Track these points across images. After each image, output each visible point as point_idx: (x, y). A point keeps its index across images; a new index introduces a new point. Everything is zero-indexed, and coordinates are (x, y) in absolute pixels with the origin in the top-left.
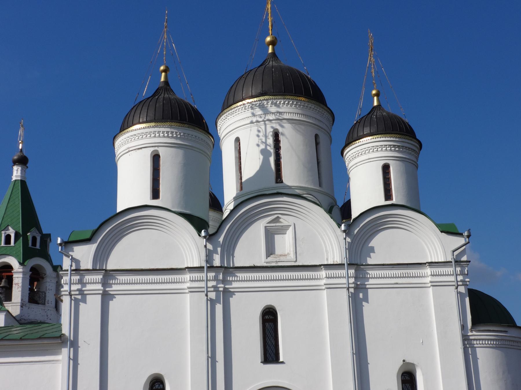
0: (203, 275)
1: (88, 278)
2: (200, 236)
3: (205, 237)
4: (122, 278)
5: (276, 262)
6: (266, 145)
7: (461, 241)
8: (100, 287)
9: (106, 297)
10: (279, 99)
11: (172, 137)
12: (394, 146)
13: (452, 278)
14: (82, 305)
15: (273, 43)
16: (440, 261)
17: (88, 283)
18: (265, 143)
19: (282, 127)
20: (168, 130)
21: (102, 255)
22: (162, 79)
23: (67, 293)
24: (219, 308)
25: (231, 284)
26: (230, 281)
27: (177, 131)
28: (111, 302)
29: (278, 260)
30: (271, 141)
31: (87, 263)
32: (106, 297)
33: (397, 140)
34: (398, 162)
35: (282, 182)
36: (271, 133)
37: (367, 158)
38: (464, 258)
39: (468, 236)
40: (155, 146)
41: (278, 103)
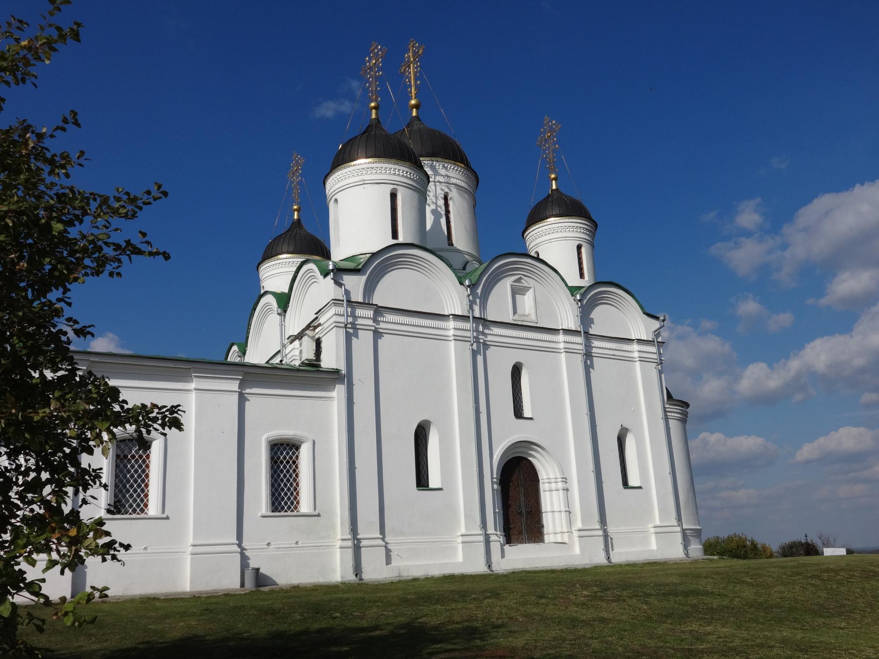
0: (468, 325)
1: (359, 312)
2: (461, 284)
3: (469, 286)
6: (437, 206)
7: (656, 324)
8: (370, 322)
9: (377, 334)
11: (410, 178)
13: (655, 356)
14: (354, 340)
15: (417, 107)
18: (436, 203)
20: (407, 170)
21: (369, 288)
22: (374, 116)
23: (343, 325)
24: (480, 359)
29: (522, 318)
30: (441, 202)
32: (377, 334)
35: (452, 245)
38: (660, 340)
39: (664, 321)
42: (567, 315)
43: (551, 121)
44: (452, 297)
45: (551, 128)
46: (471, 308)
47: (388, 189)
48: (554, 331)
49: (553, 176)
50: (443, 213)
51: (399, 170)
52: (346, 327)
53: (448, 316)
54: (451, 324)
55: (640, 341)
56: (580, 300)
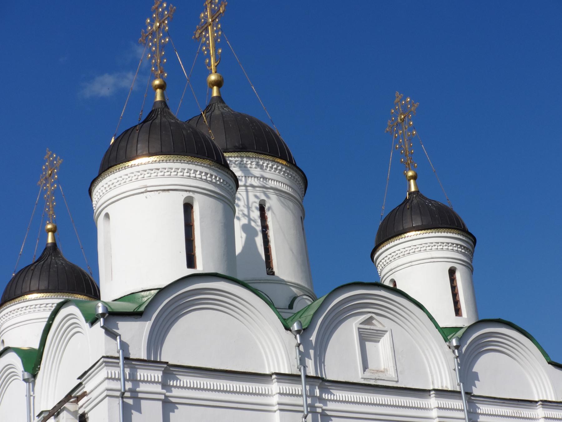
0: (298, 388)
1: (142, 374)
2: (287, 328)
3: (298, 332)
4: (186, 380)
5: (376, 379)
6: (250, 219)
8: (158, 388)
10: (266, 160)
11: (211, 182)
12: (461, 246)
15: (218, 84)
16: (550, 399)
17: (143, 381)
18: (248, 216)
19: (268, 197)
20: (207, 170)
21: (156, 339)
22: (158, 98)
23: (118, 394)
25: (326, 405)
26: (325, 399)
27: (216, 175)
28: (171, 414)
29: (376, 376)
30: (256, 214)
31: (139, 351)
32: (168, 406)
33: (464, 239)
34: (464, 267)
35: (273, 274)
36: (258, 206)
37: (430, 256)
40: (190, 191)
41: (265, 165)
42: (440, 369)
43: (404, 98)
44: (273, 347)
45: (405, 107)
46: (302, 362)
47: (179, 198)
48: (422, 392)
49: (410, 174)
50: (259, 229)
51: (195, 171)
52: (122, 396)
53: (270, 375)
54: (275, 387)
55: (546, 403)
56: (457, 347)
